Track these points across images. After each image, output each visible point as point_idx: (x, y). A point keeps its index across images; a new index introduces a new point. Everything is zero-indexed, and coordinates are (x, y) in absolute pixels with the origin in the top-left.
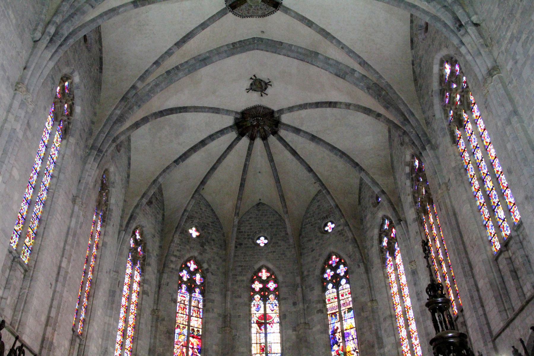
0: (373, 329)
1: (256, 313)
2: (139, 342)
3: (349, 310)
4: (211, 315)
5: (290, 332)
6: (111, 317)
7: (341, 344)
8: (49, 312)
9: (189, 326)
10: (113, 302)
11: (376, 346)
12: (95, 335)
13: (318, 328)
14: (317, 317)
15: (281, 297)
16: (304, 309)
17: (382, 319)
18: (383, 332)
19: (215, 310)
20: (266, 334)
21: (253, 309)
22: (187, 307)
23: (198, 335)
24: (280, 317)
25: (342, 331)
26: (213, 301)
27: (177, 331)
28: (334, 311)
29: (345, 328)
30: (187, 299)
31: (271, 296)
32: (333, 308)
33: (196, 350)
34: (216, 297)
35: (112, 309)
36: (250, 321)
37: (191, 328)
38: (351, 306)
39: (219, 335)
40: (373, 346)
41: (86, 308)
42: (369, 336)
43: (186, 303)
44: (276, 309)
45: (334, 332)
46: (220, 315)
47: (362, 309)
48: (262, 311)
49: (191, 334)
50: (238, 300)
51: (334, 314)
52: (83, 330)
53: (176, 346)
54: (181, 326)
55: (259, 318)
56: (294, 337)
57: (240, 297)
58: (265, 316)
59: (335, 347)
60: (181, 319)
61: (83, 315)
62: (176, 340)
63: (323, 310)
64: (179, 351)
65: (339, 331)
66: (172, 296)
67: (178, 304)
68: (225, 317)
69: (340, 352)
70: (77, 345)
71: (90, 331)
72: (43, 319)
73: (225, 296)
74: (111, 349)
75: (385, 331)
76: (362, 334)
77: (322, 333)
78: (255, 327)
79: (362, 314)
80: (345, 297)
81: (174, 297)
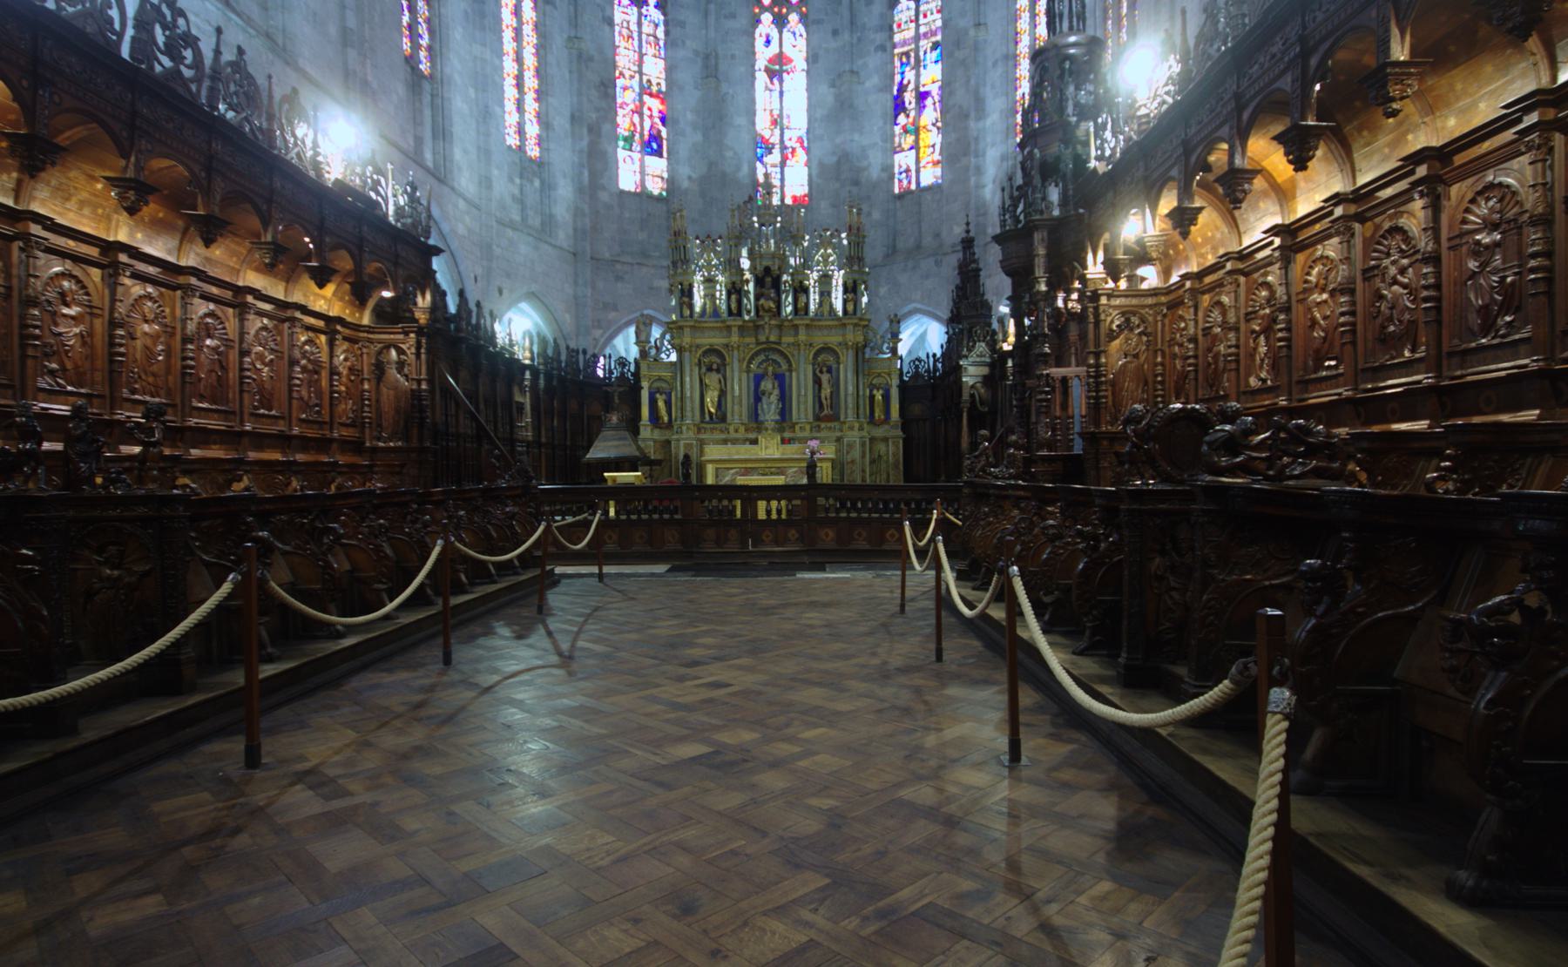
0: (973, 82)
1: (763, 55)
2: (550, 100)
3: (935, 46)
4: (681, 53)
5: (824, 89)
6: (484, 45)
7: (912, 114)
8: (343, 18)
9: (641, 73)
10: (482, 15)
11: (973, 114)
12: (457, 77)
13: (874, 81)
14: (874, 60)
15: (811, 17)
16: (852, 45)
17: (990, 64)
18: (988, 88)
19: (688, 43)
20: (781, 93)
21: (759, 42)
22: (635, 35)
23: (659, 92)
24: (807, 60)
25: (917, 88)
26: (682, 24)
27: (620, 83)
28: (905, 49)
29: (923, 80)
30: (634, 19)
31: (793, 18)
32: (904, 43)
33: (657, 120)
34: (691, 18)
35: (483, 28)
36: (753, 66)
37: (645, 78)
38: (939, 38)
39: (698, 94)
40: (967, 116)
41: (428, 21)
42: (961, 97)
43: (634, 27)
44: (802, 43)
45: (902, 88)
46: (696, 53)
47: (958, 44)
48: (774, 49)
49: (645, 90)
50: (731, 24)
51: (907, 54)
52: (433, 67)
53: (620, 112)
54: (627, 74)
55: (770, 61)
56: (830, 99)
57: (733, 16)
58: (781, 59)
59: (902, 119)
60: (625, 58)
61: (426, 36)
62: (619, 100)
63: (887, 46)
64: (627, 120)
65: (911, 86)
66: (603, 10)
67: (617, 29)
68: (707, 57)
69: (910, 127)
70: (427, 99)
71: (447, 70)
72: (333, 30)
73: (706, 14)
74: (497, 109)
75: (993, 87)
76: (951, 93)
77: (881, 90)
78: (761, 78)
79: (957, 54)
80: (930, 18)
81: (608, 13)
